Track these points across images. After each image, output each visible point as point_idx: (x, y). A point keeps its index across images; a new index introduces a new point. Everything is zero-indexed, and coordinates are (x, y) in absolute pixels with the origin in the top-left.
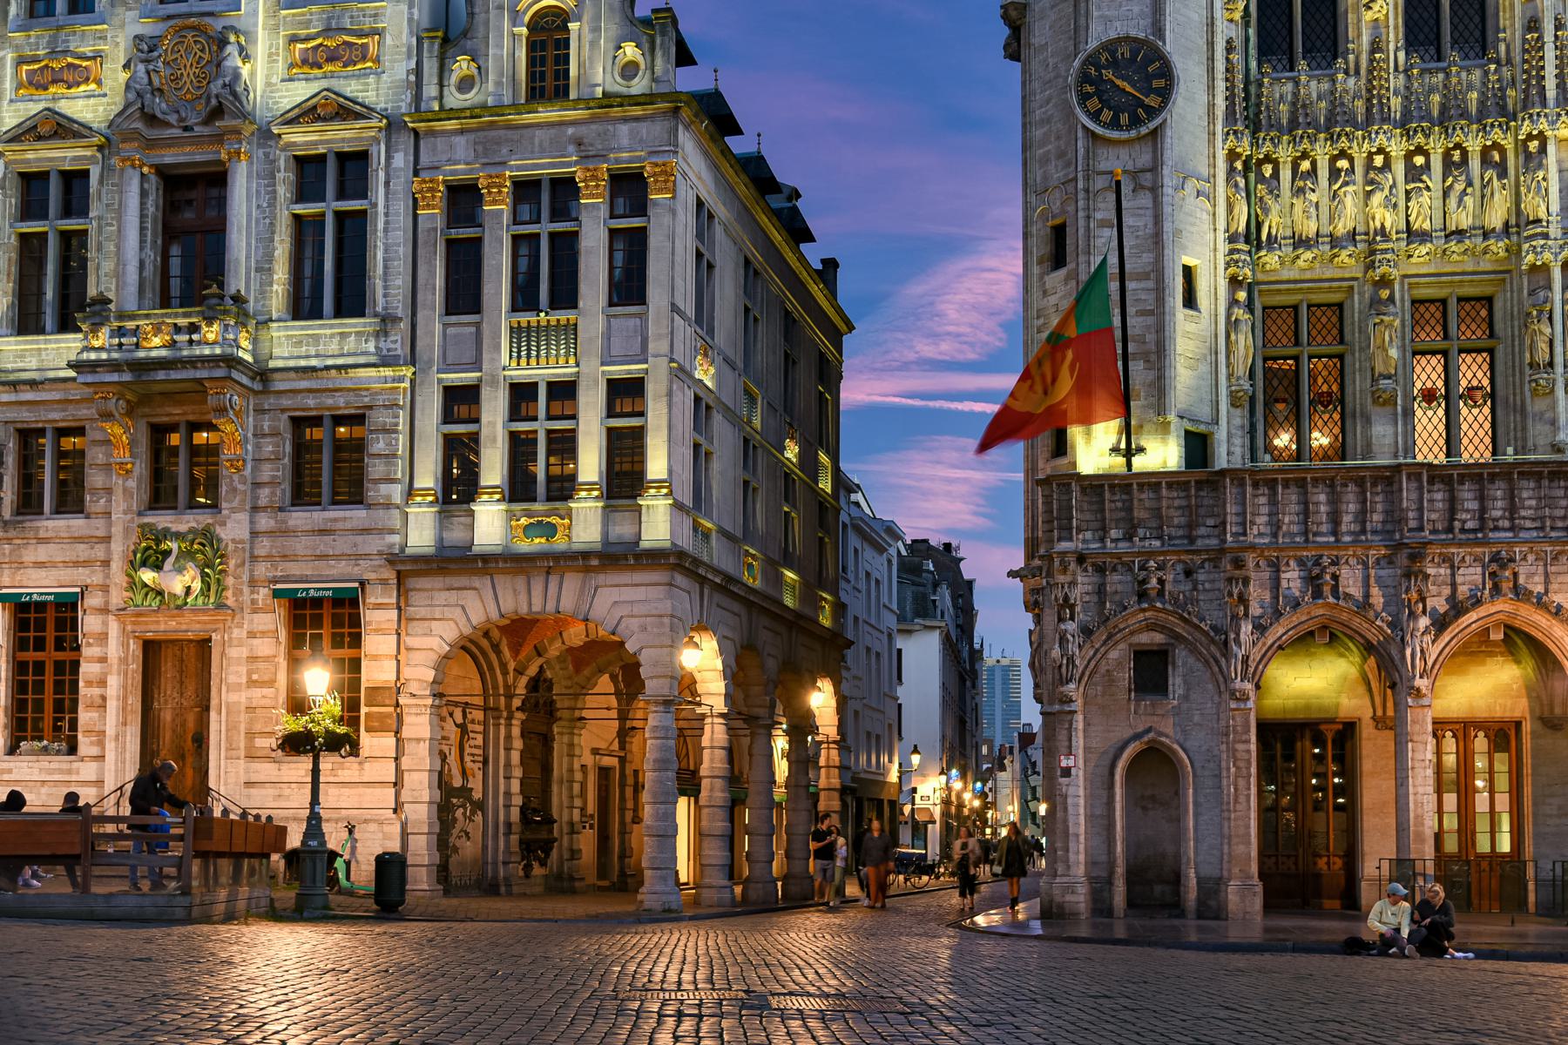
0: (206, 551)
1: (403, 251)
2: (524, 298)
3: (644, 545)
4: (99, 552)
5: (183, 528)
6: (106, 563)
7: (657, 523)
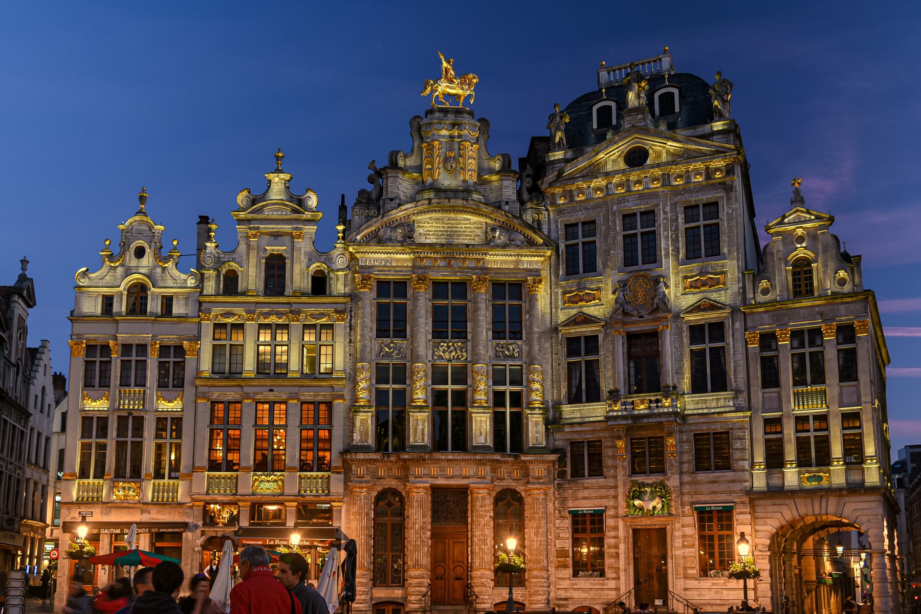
0: (662, 491)
1: (742, 363)
2: (799, 380)
3: (867, 484)
4: (612, 492)
5: (650, 482)
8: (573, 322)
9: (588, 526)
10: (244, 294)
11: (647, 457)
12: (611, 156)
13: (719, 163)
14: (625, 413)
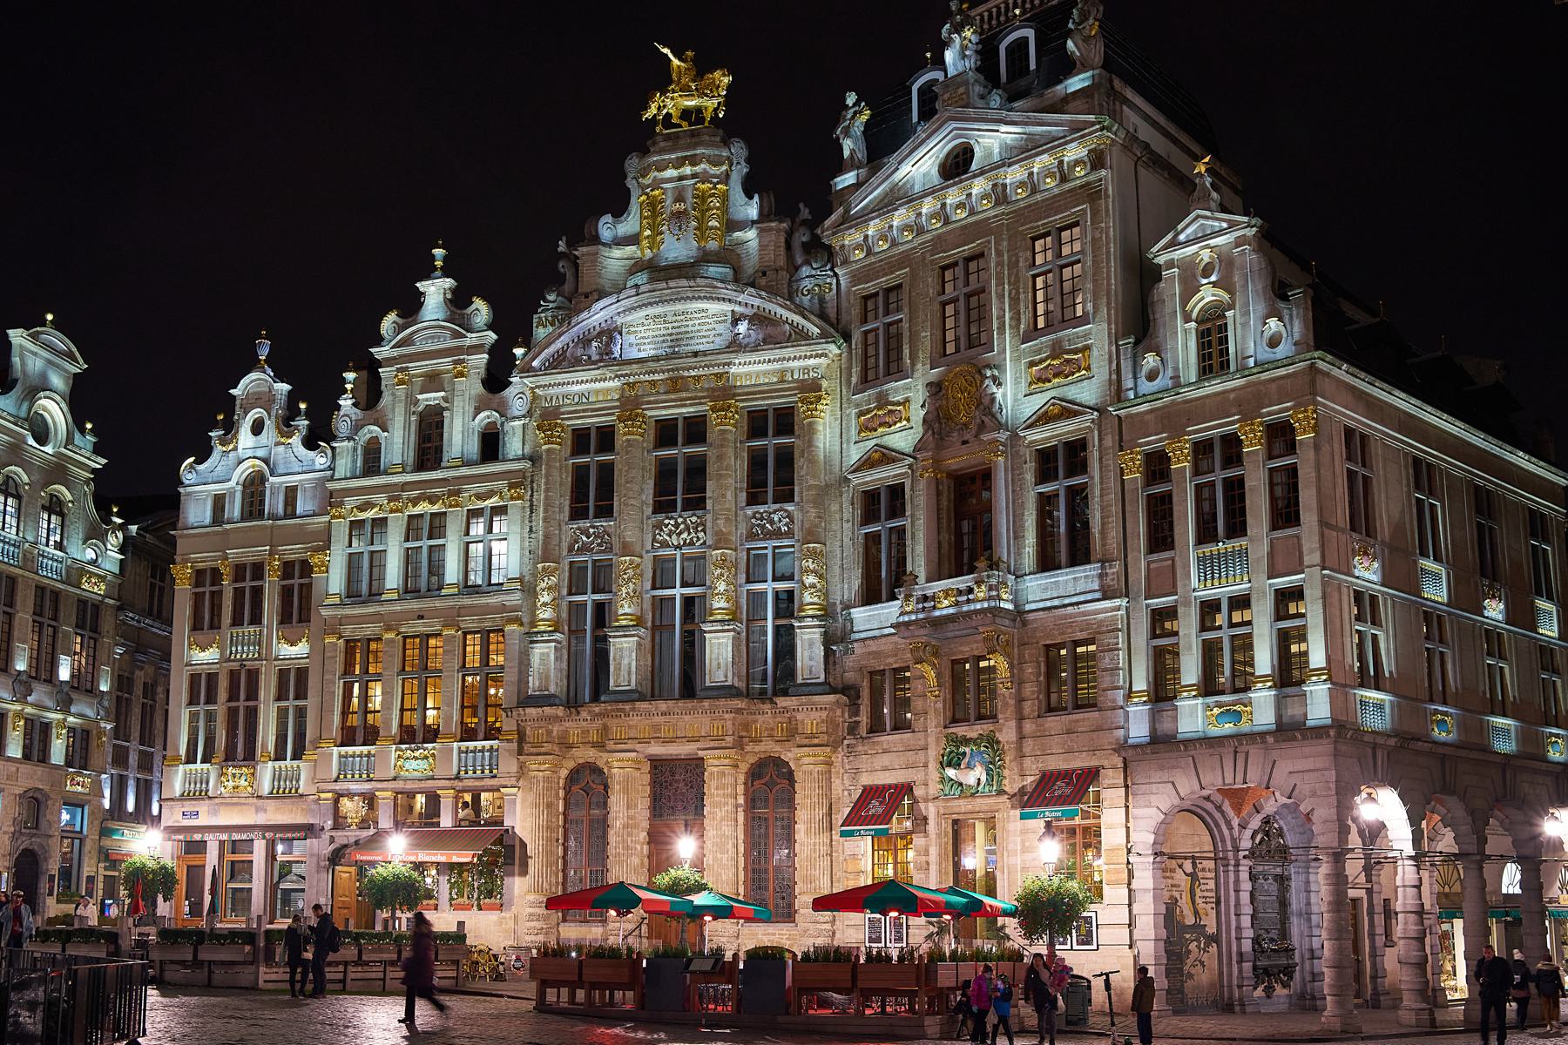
1: (1115, 509)
2: (1206, 534)
3: (1310, 723)
4: (921, 756)
5: (974, 735)
6: (926, 766)
7: (1318, 703)
8: (867, 463)
10: (386, 473)
12: (919, 165)
13: (1074, 152)
14: (921, 616)
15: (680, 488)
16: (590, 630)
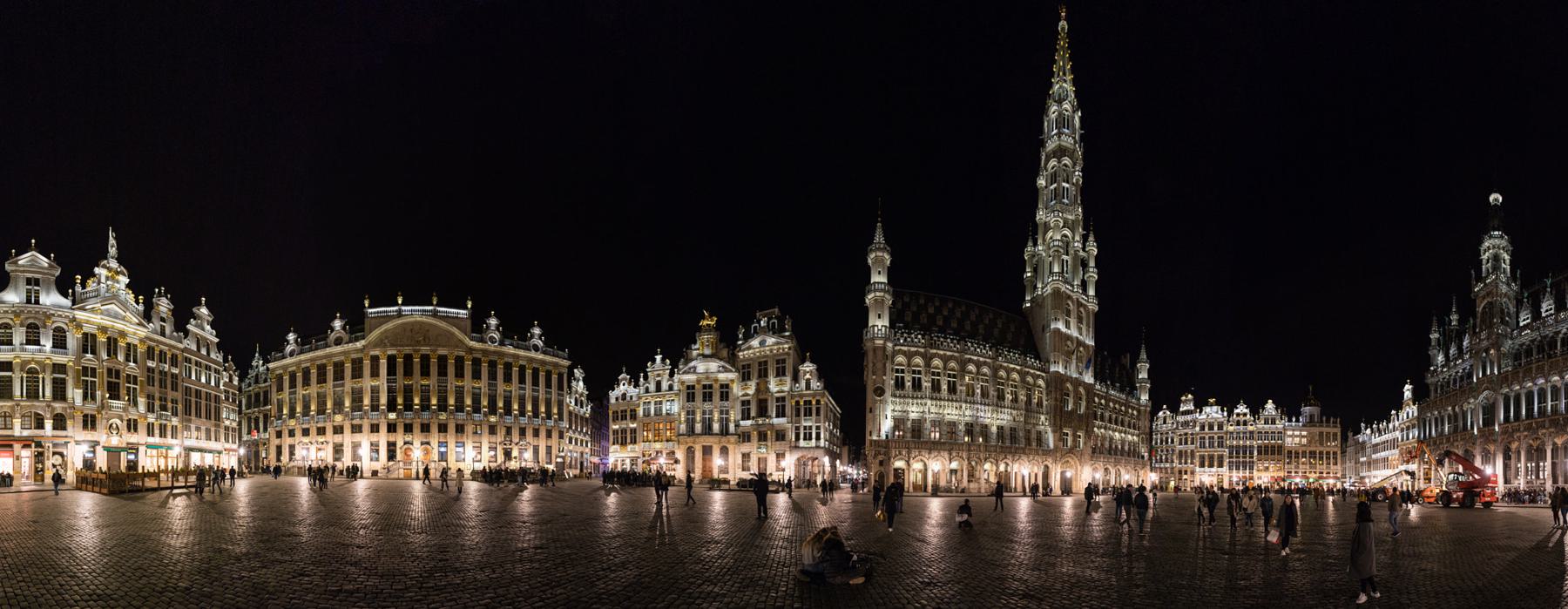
7: (822, 443)
9: (746, 456)
11: (763, 437)
12: (755, 343)
15: (708, 397)
16: (691, 424)
